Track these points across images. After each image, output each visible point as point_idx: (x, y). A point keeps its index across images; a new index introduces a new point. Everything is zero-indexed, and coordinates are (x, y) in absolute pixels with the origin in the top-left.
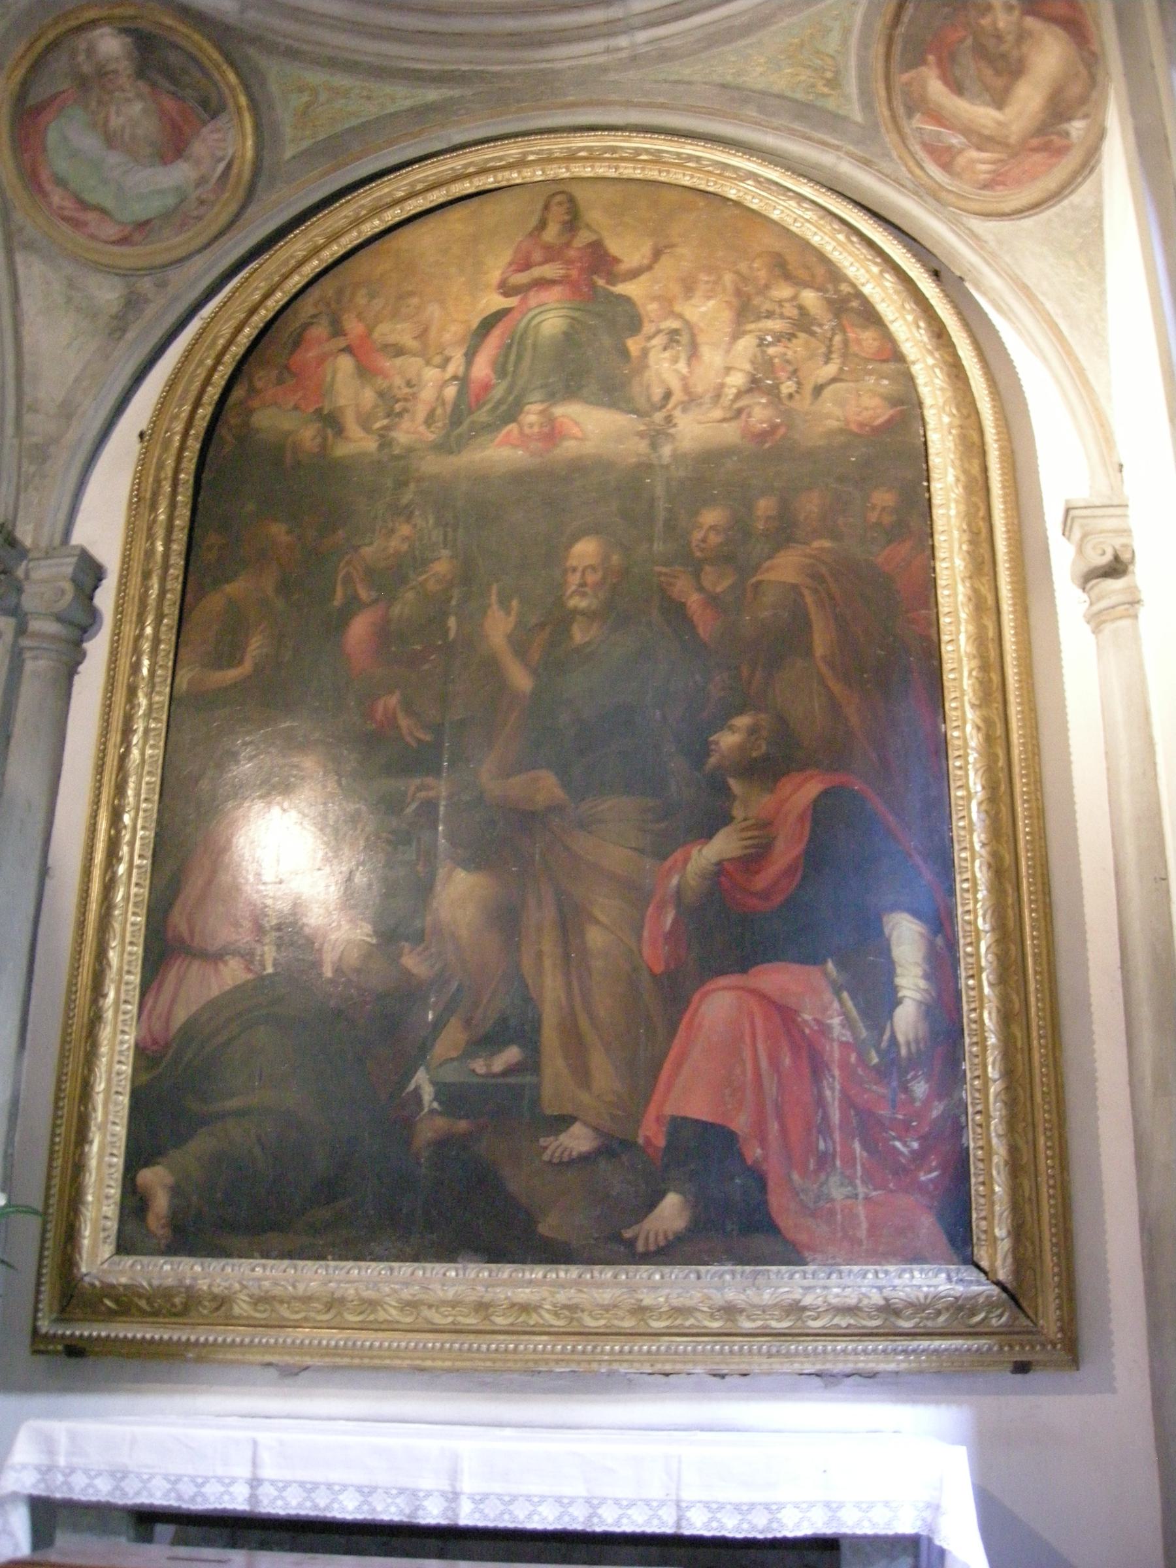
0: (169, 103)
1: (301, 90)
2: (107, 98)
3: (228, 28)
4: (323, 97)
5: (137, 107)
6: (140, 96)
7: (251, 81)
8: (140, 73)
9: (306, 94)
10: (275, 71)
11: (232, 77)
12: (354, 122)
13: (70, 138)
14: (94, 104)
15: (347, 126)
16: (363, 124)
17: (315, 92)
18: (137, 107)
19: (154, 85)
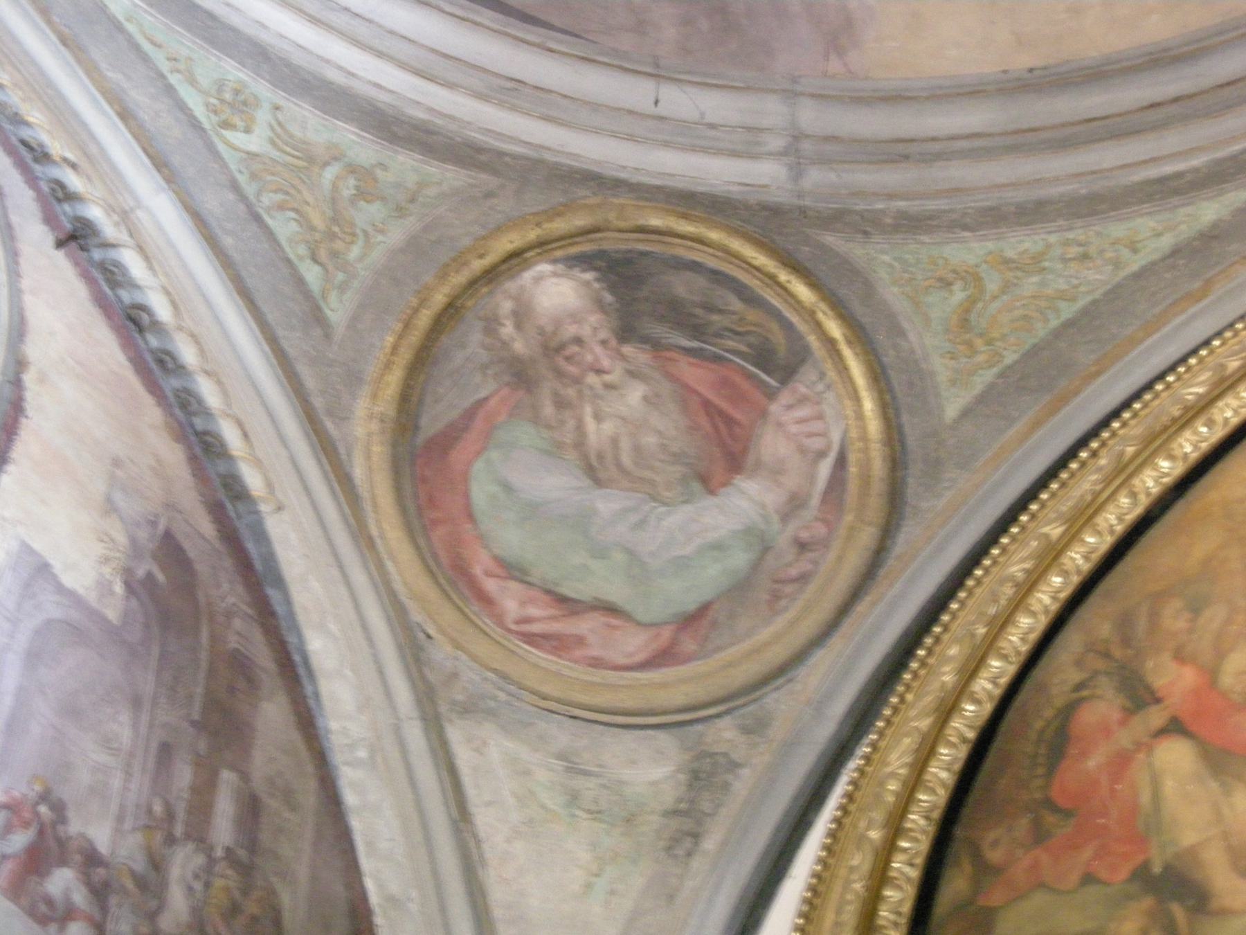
0: (695, 374)
1: (946, 284)
2: (571, 392)
3: (775, 211)
4: (992, 286)
5: (635, 394)
6: (633, 374)
7: (843, 290)
8: (626, 332)
9: (957, 286)
10: (882, 260)
11: (803, 291)
12: (1068, 311)
13: (518, 484)
14: (548, 410)
15: (1054, 323)
16: (1085, 312)
17: (973, 278)
18: (635, 394)
19: (656, 346)
